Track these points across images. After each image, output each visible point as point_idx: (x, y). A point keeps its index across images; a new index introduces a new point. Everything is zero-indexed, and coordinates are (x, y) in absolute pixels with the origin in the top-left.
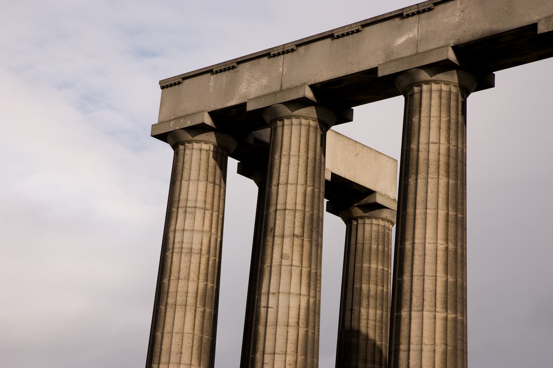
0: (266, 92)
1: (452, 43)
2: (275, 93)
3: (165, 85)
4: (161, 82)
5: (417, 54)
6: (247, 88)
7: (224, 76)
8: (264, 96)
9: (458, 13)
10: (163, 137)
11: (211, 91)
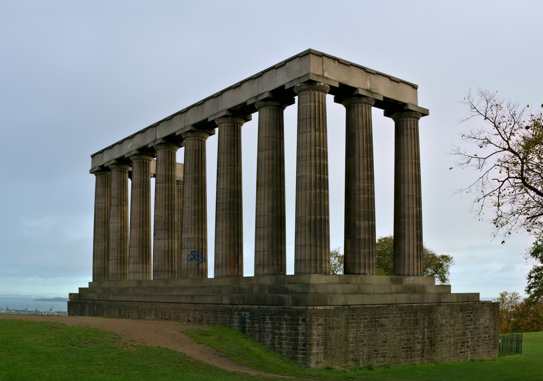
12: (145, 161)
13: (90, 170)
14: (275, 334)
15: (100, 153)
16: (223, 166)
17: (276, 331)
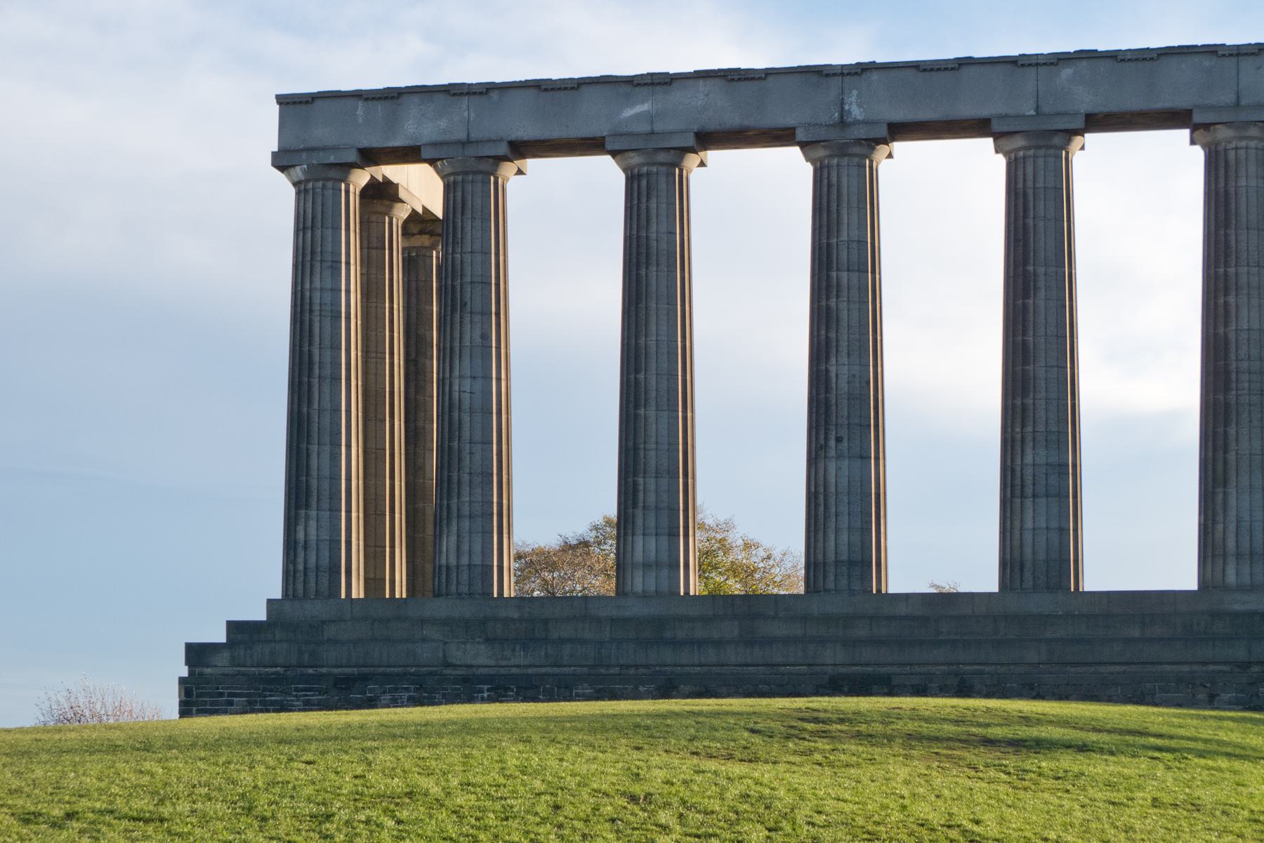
0: (447, 137)
1: (696, 128)
2: (465, 143)
3: (285, 102)
5: (652, 133)
6: (417, 128)
7: (380, 107)
11: (360, 120)
13: (273, 153)
15: (367, 99)
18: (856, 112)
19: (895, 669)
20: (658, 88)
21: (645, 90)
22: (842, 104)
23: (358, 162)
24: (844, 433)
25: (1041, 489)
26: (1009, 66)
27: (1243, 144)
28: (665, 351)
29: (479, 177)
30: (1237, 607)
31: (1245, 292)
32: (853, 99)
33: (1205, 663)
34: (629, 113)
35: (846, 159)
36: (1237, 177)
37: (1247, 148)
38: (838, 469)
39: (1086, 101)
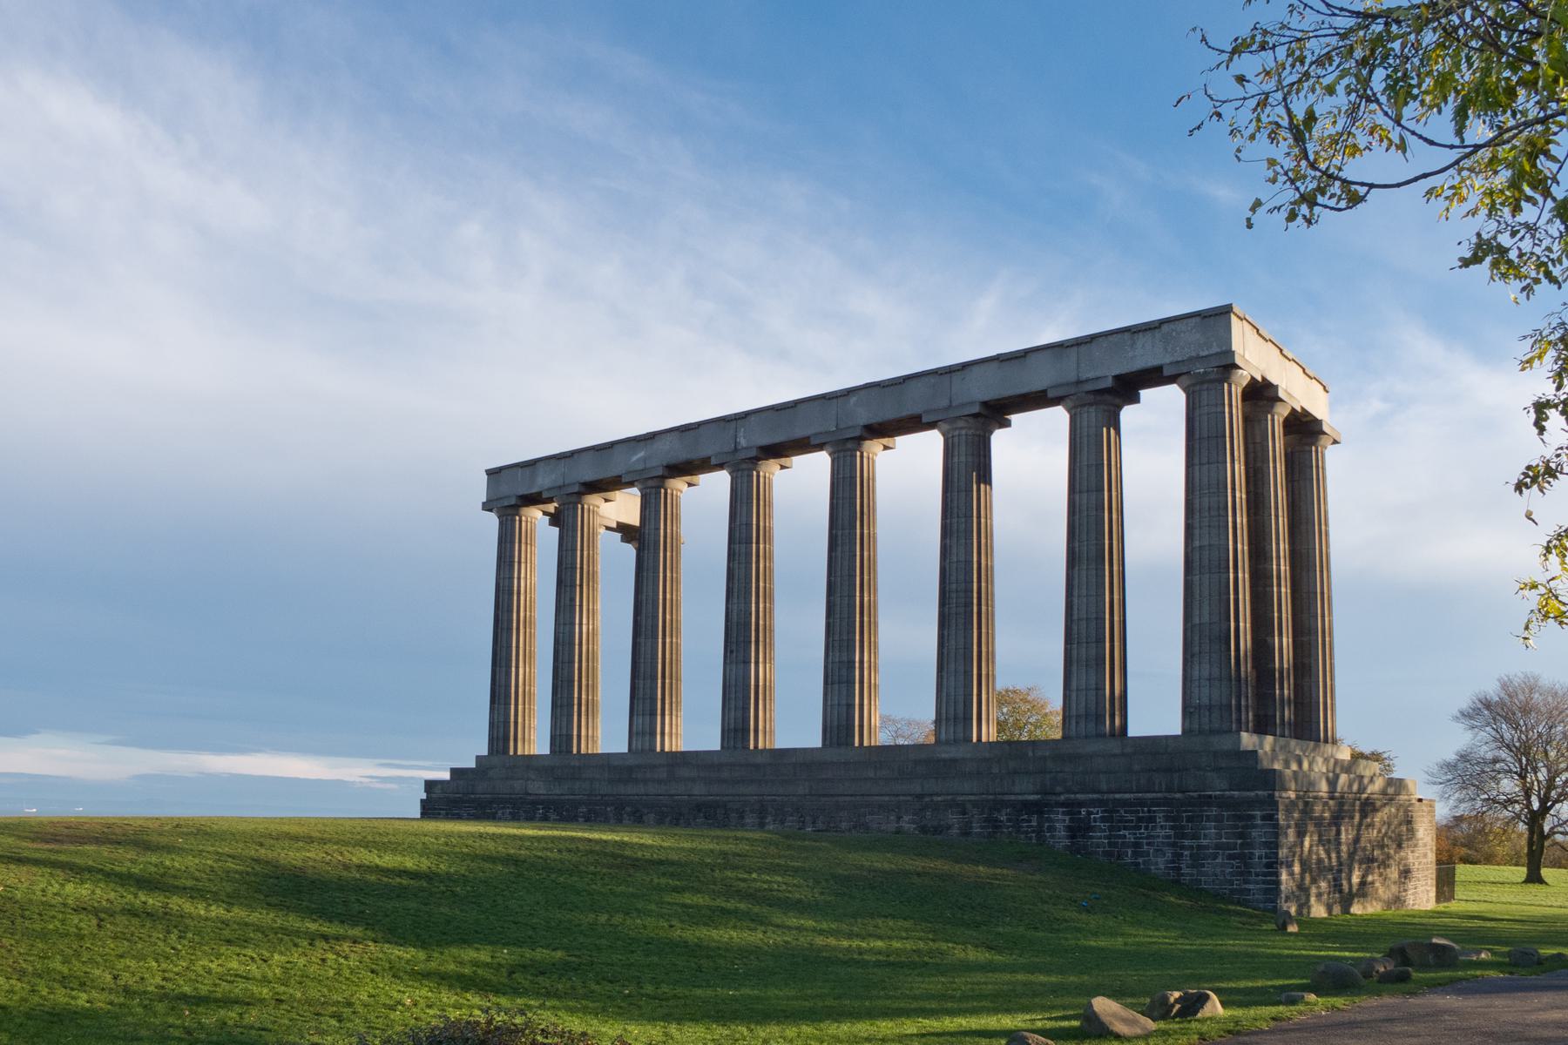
3: (490, 473)
4: (486, 471)
7: (527, 471)
8: (553, 488)
9: (668, 443)
10: (491, 510)
12: (675, 492)
13: (484, 503)
14: (1183, 847)
15: (522, 467)
16: (966, 517)
17: (1186, 842)
18: (743, 442)
19: (731, 798)
20: (649, 441)
21: (642, 444)
22: (736, 438)
23: (519, 503)
24: (734, 648)
25: (836, 678)
26: (823, 400)
27: (957, 433)
28: (651, 602)
29: (571, 506)
30: (944, 756)
31: (956, 535)
32: (742, 434)
33: (898, 795)
34: (634, 458)
35: (740, 473)
36: (952, 456)
37: (959, 435)
38: (731, 670)
39: (864, 417)
